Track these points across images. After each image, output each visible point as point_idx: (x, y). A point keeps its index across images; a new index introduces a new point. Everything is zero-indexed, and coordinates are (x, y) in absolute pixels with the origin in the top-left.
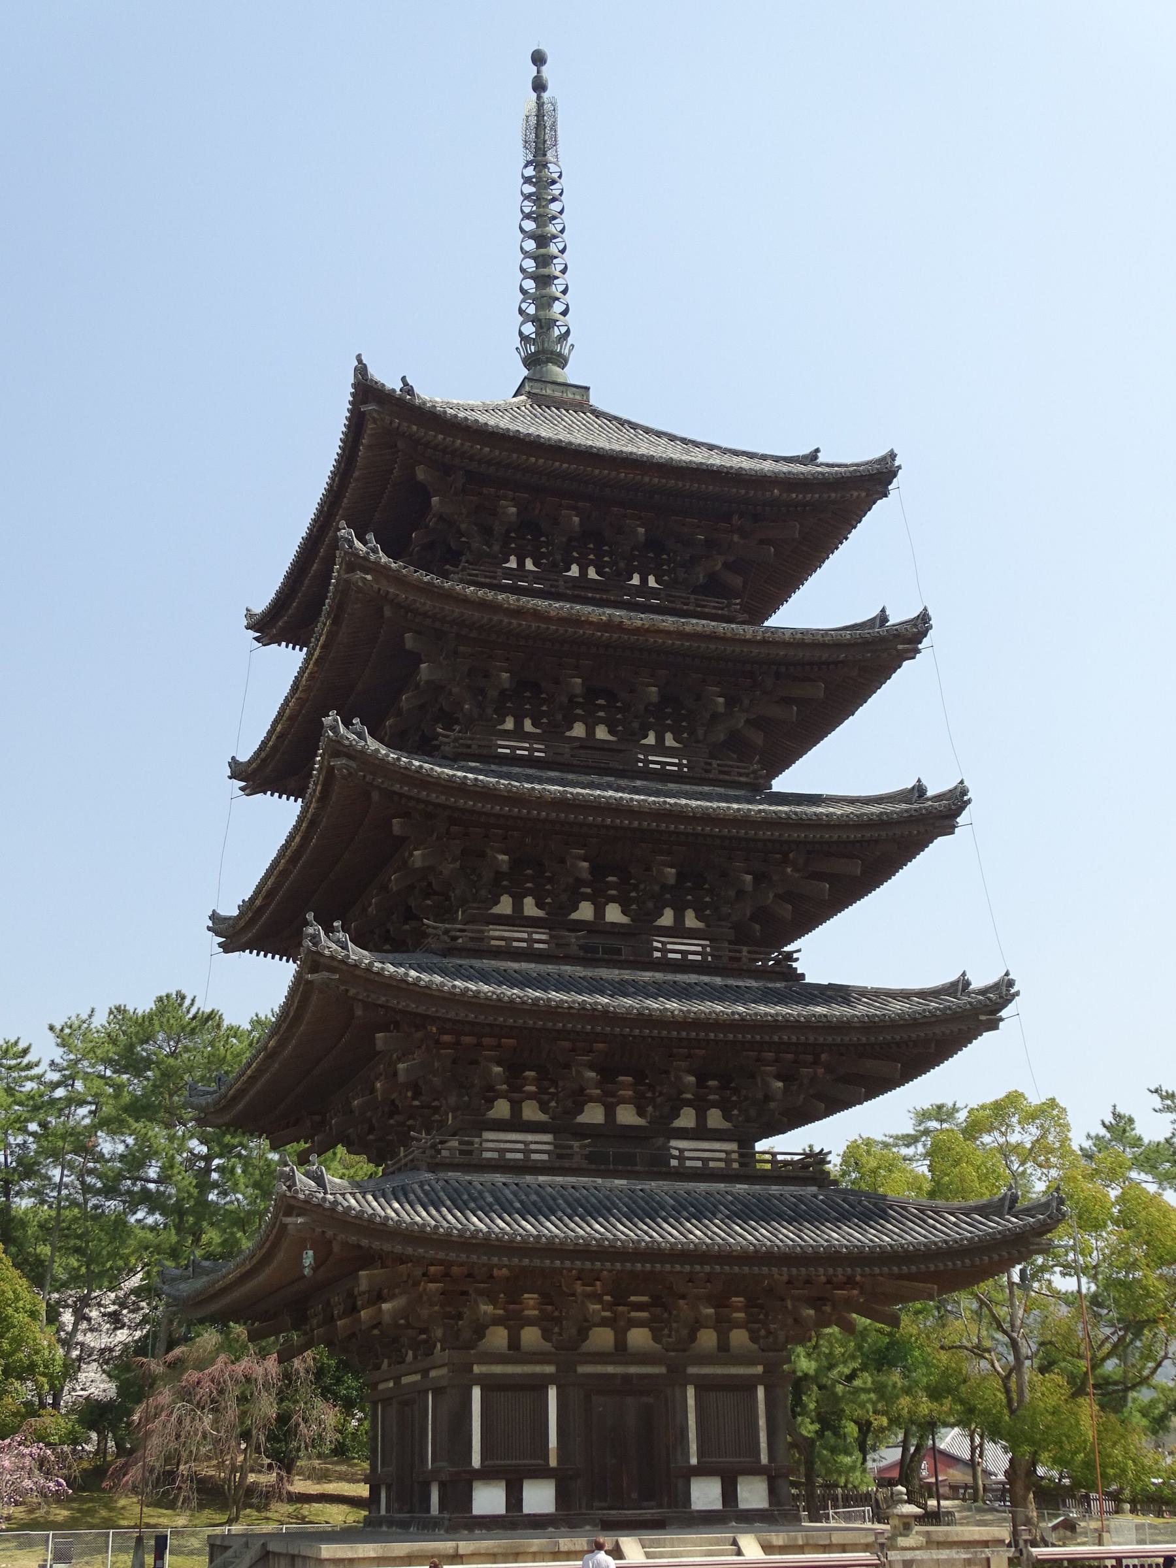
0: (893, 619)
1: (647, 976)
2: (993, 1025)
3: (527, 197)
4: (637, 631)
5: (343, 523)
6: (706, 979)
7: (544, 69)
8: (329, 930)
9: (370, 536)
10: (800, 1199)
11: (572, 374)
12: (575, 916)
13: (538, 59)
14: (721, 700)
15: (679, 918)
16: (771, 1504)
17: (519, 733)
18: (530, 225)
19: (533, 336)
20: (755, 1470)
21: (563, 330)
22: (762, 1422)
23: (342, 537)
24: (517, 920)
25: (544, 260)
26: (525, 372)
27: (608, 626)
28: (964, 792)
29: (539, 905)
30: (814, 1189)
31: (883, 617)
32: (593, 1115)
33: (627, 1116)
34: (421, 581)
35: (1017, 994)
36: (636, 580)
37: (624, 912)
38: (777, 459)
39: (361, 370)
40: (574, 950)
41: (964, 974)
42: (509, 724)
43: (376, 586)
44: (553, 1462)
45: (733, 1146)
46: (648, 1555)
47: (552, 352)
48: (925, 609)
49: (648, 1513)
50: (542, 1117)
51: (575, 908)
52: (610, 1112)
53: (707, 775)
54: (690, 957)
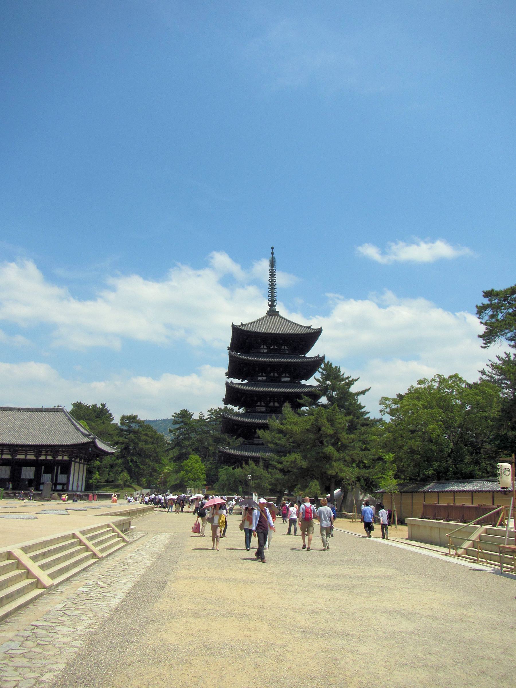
0: (320, 357)
12: (270, 405)
13: (273, 248)
24: (261, 406)
29: (264, 403)
31: (318, 356)
36: (283, 348)
42: (260, 374)
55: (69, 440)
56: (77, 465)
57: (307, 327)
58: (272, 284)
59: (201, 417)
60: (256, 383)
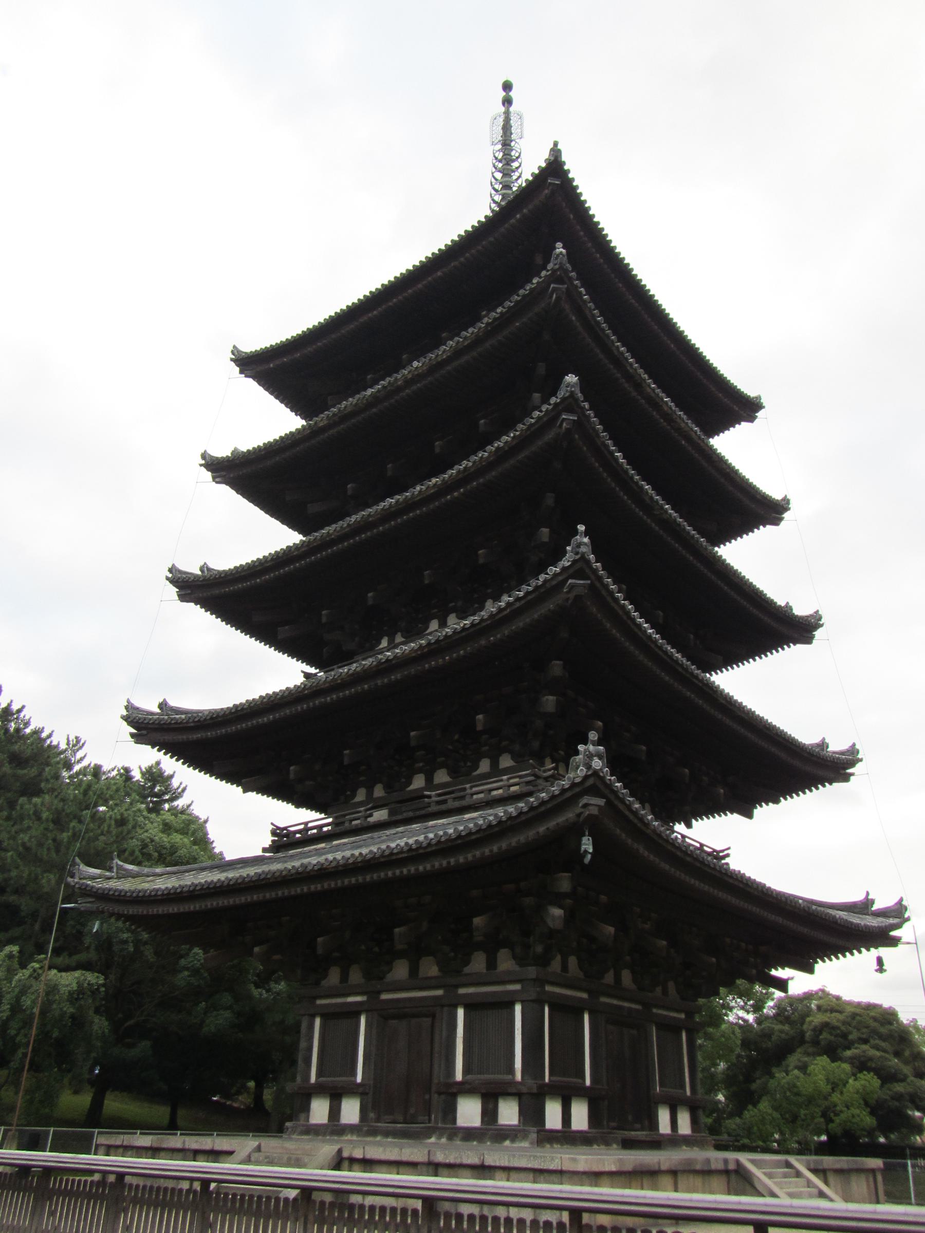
2: (846, 778)
4: (679, 430)
5: (559, 245)
13: (507, 87)
16: (693, 1130)
23: (561, 253)
27: (669, 418)
28: (820, 618)
34: (594, 316)
35: (861, 760)
39: (556, 152)
44: (588, 1082)
49: (640, 1135)
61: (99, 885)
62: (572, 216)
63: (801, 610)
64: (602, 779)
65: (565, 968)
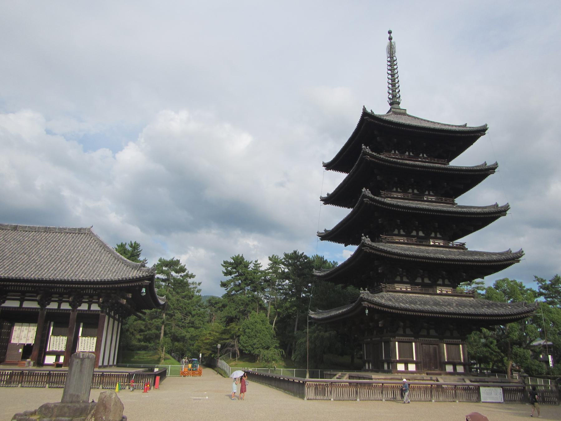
0: (488, 165)
1: (431, 248)
2: (518, 261)
3: (389, 66)
5: (363, 145)
6: (444, 249)
7: (392, 35)
8: (366, 238)
9: (368, 147)
10: (469, 300)
11: (402, 106)
12: (412, 234)
13: (390, 32)
14: (446, 184)
15: (436, 235)
16: (464, 371)
17: (397, 192)
18: (389, 72)
19: (391, 98)
20: (460, 364)
21: (398, 96)
22: (461, 352)
24: (399, 235)
25: (393, 80)
26: (390, 107)
29: (404, 231)
30: (472, 299)
31: (485, 164)
32: (419, 280)
33: (427, 281)
34: (380, 157)
35: (524, 254)
36: (421, 155)
37: (423, 233)
38: (456, 126)
39: (364, 109)
40: (414, 243)
41: (510, 249)
42: (395, 190)
43: (370, 159)
44: (415, 359)
45: (451, 288)
46: (444, 381)
47: (397, 102)
48: (496, 162)
49: (437, 371)
50: (408, 281)
51: (412, 232)
52: (423, 280)
53: (442, 201)
54: (441, 244)
55: (105, 273)
56: (111, 320)
57: (459, 126)
58: (393, 75)
59: (257, 265)
60: (393, 200)
61: (312, 316)
62: (376, 122)
63: (501, 204)
64: (364, 298)
65: (404, 332)
